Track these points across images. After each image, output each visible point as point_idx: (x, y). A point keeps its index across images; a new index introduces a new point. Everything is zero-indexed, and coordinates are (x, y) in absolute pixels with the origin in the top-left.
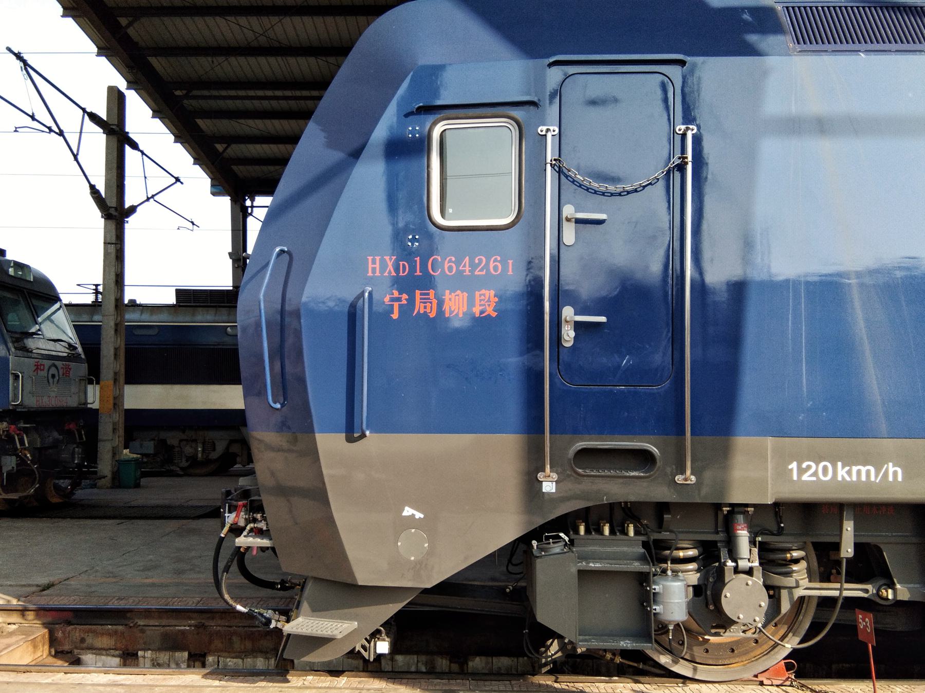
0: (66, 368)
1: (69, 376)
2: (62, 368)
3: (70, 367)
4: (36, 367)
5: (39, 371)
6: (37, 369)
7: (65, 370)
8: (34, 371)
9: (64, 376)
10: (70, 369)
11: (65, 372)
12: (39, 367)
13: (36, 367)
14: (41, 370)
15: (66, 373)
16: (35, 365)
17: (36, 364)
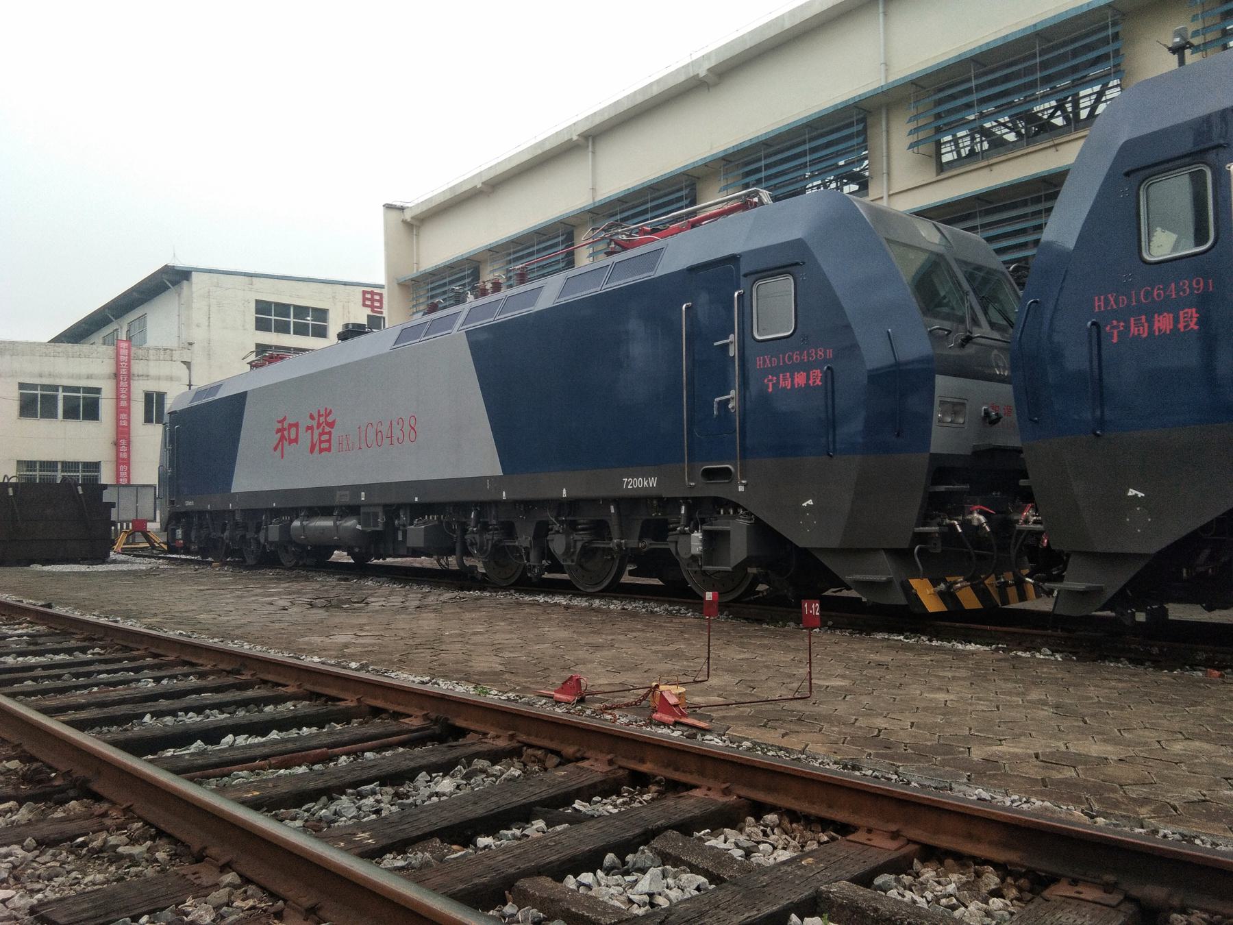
0: (319, 425)
1: (329, 450)
2: (308, 428)
3: (330, 419)
4: (279, 434)
5: (286, 443)
6: (283, 437)
7: (316, 432)
8: (275, 449)
9: (317, 448)
10: (332, 425)
11: (316, 437)
12: (286, 433)
13: (279, 434)
14: (291, 441)
15: (321, 442)
16: (278, 431)
17: (279, 426)
